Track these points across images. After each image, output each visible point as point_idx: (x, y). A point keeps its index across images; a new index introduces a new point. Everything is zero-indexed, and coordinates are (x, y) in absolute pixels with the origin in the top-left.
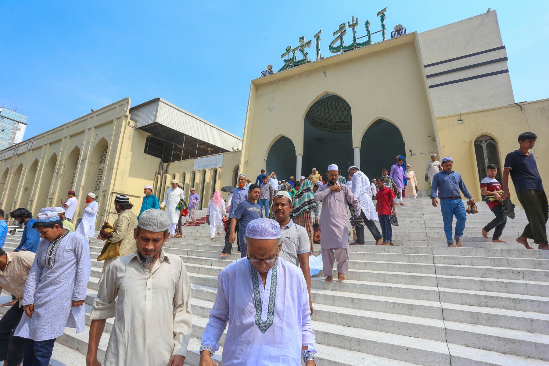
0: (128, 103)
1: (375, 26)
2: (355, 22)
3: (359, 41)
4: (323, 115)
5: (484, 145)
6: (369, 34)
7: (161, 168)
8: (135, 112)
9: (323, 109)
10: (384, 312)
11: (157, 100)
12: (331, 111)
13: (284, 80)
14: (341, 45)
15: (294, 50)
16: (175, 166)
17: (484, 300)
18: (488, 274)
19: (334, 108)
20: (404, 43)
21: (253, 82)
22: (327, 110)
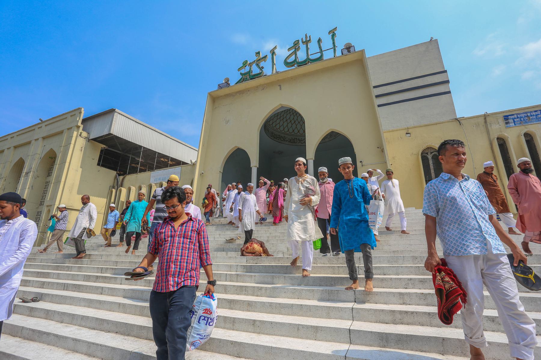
0: (80, 113)
1: (327, 43)
2: (308, 39)
3: (311, 57)
4: (282, 128)
5: (430, 157)
6: (321, 51)
7: (116, 181)
8: (89, 123)
9: (281, 123)
10: (287, 336)
11: (112, 111)
12: (290, 125)
13: (241, 92)
14: (295, 60)
15: (251, 65)
16: (130, 178)
17: (399, 316)
18: (410, 285)
19: (293, 122)
20: (354, 61)
21: (210, 94)
22: (285, 124)
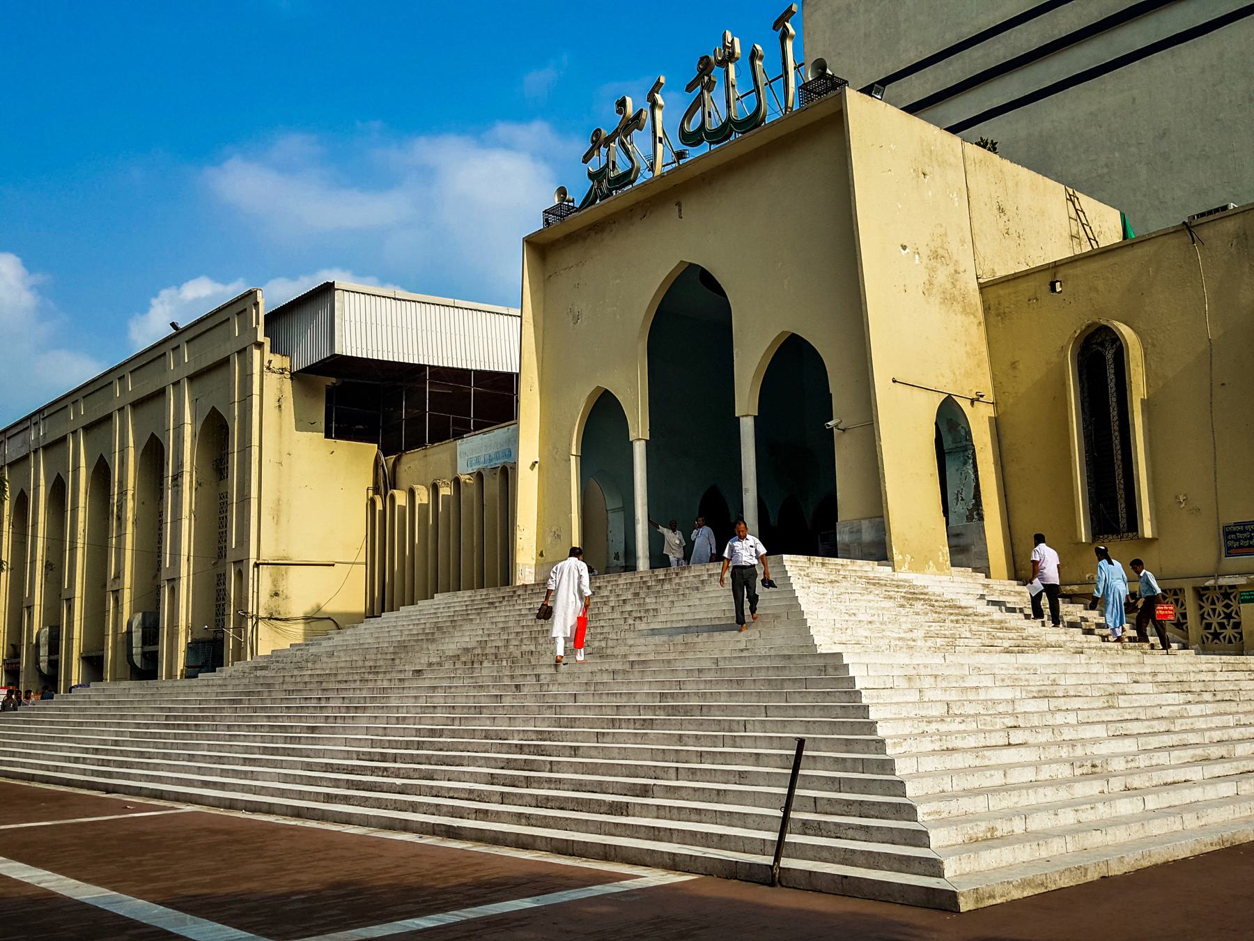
0: (256, 304)
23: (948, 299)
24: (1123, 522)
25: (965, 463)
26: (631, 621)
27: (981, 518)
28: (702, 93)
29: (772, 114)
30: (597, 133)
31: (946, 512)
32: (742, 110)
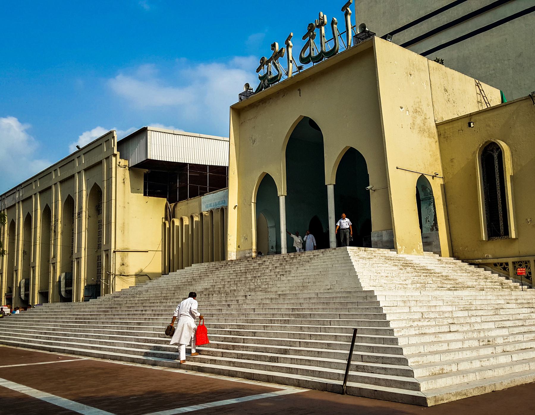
0: (113, 137)
11: (144, 131)
23: (422, 131)
24: (502, 231)
25: (430, 205)
26: (279, 276)
27: (437, 230)
28: (310, 40)
29: (341, 47)
30: (263, 59)
31: (421, 227)
32: (328, 47)
